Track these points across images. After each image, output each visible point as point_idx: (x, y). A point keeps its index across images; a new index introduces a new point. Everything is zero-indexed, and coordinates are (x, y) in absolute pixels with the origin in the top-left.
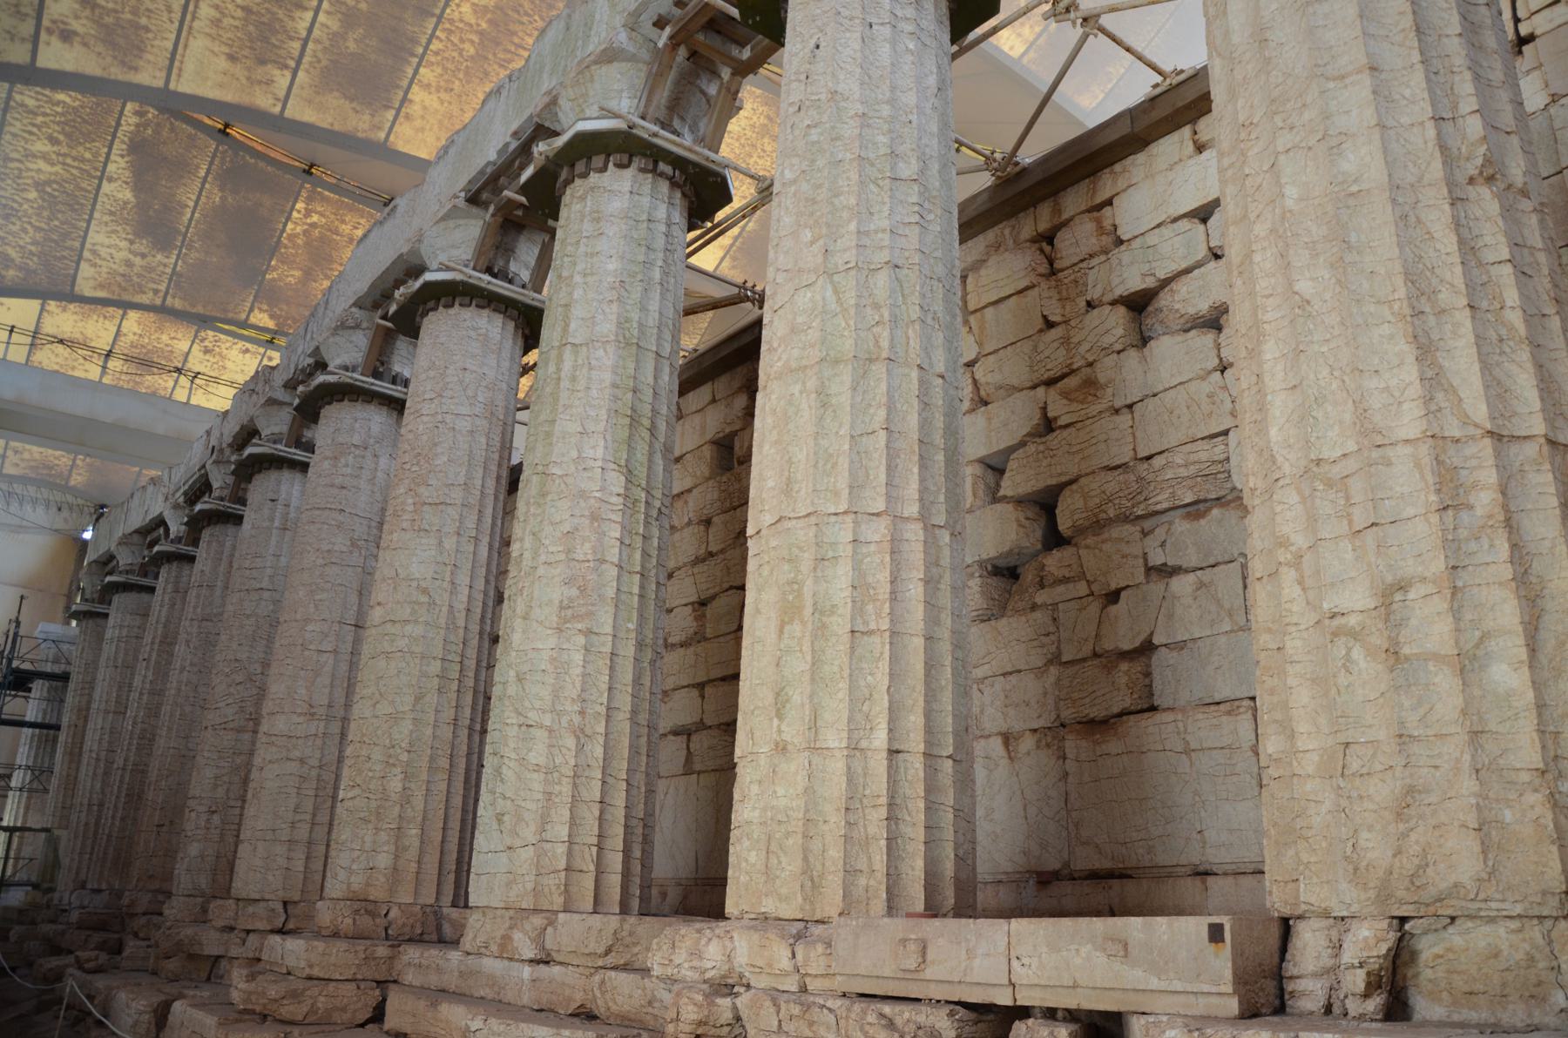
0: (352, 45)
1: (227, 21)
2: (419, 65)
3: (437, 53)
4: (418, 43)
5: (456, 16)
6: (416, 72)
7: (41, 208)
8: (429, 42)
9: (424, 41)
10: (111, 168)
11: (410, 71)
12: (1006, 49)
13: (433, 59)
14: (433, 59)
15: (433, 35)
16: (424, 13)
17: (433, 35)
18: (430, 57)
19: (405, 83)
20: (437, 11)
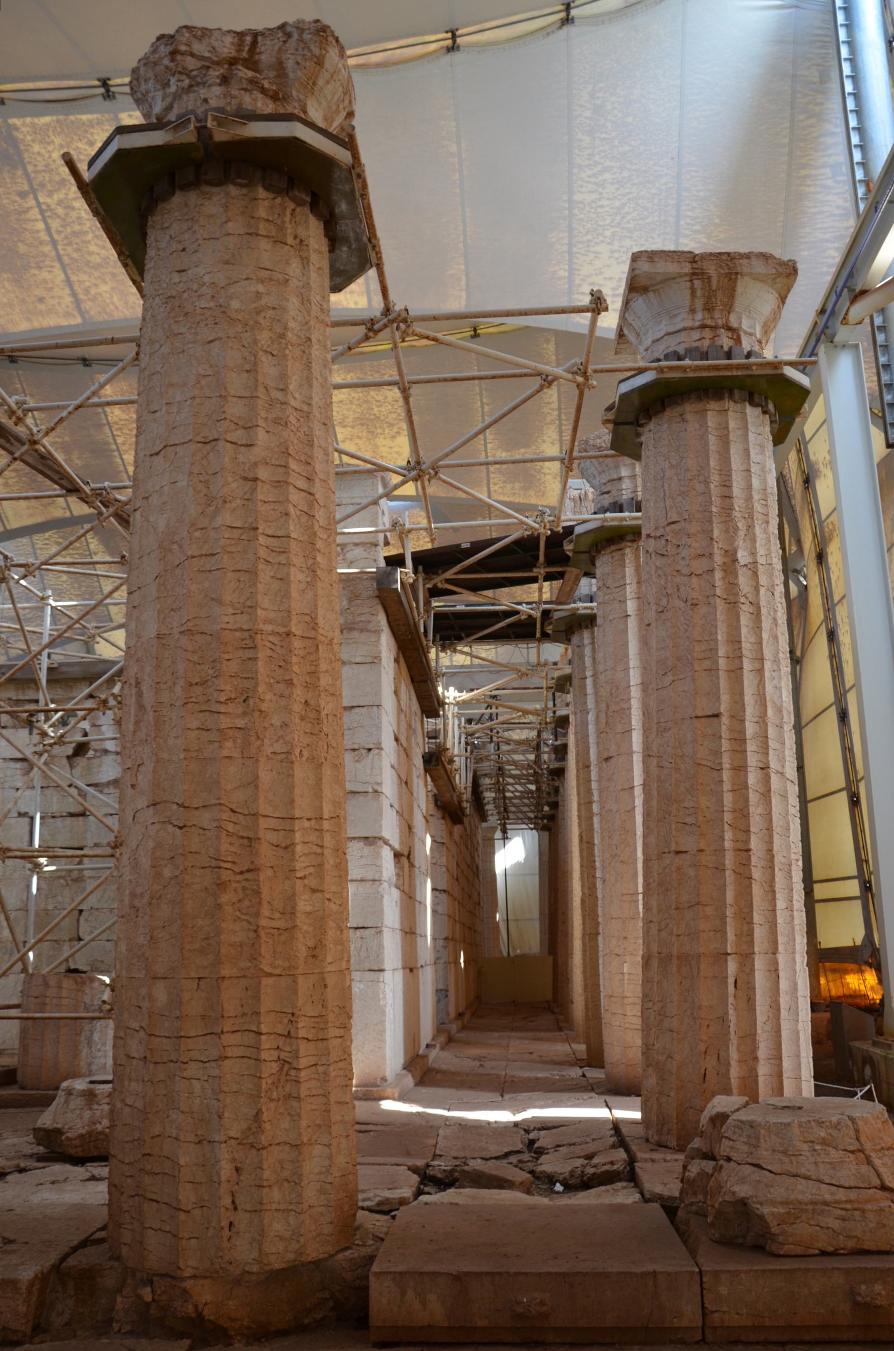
0: (77, 462)
1: (11, 481)
2: (120, 455)
3: (124, 444)
4: (108, 443)
5: (116, 419)
6: (122, 460)
7: (72, 583)
8: (115, 441)
9: (112, 441)
10: (92, 546)
11: (119, 460)
12: (352, 306)
13: (125, 448)
14: (125, 448)
15: (114, 436)
16: (99, 426)
17: (114, 436)
18: (122, 448)
19: (122, 468)
20: (105, 421)
